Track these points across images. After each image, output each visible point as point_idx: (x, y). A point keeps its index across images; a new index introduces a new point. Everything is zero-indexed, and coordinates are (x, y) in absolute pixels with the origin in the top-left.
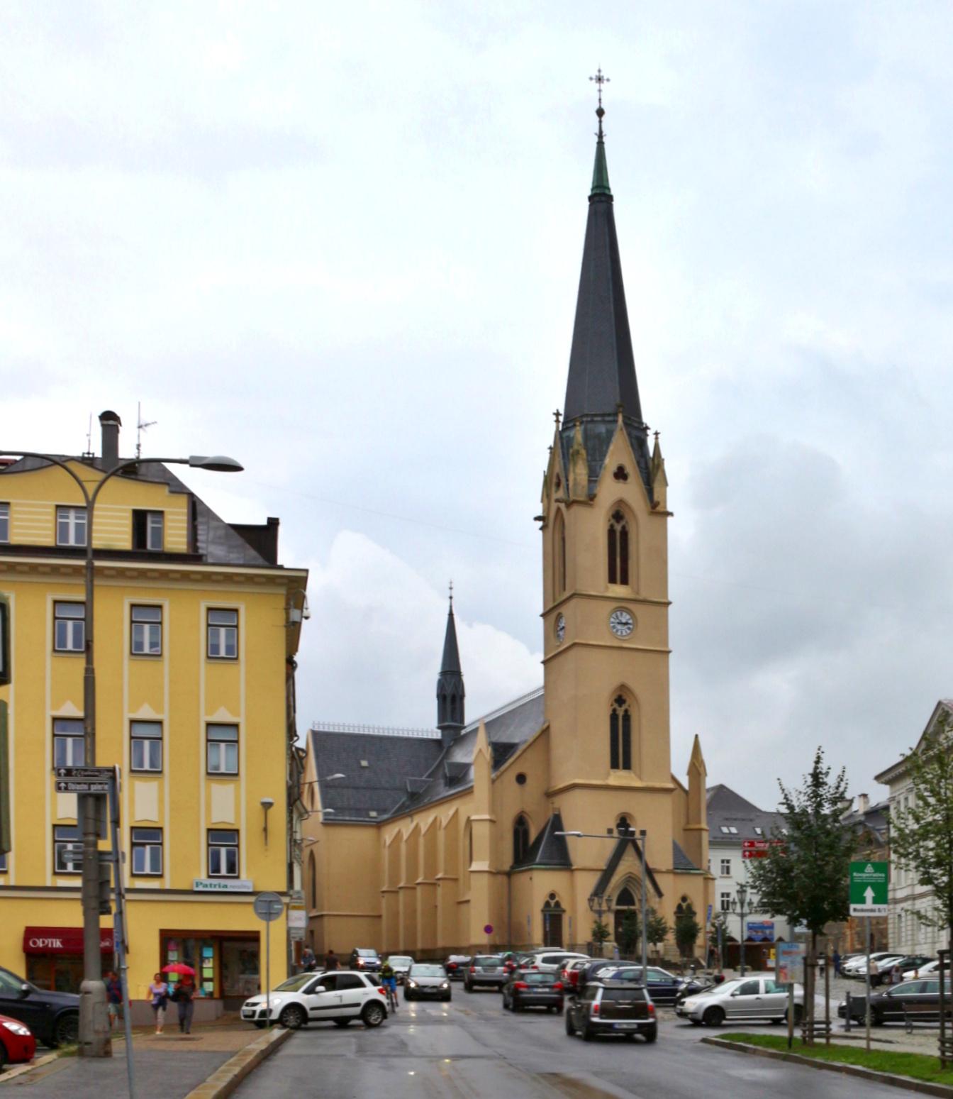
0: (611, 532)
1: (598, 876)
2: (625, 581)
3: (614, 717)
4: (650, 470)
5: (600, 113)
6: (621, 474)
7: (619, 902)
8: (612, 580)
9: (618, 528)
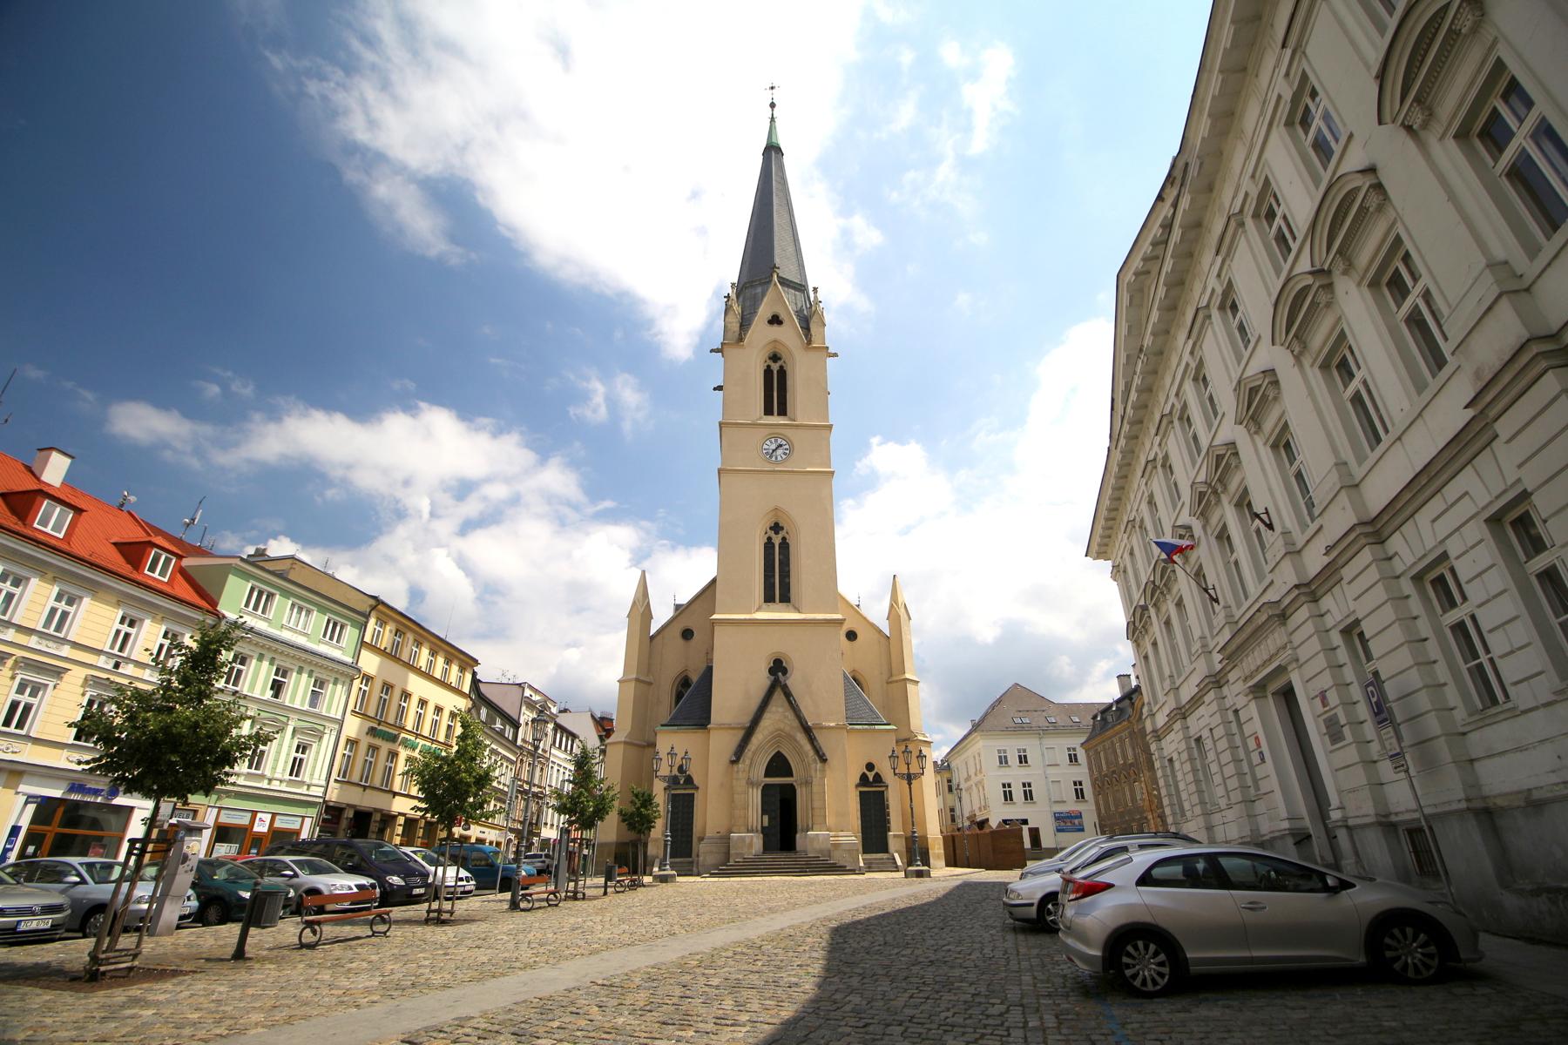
0: (768, 372)
1: (741, 734)
2: (783, 412)
3: (769, 546)
4: (809, 320)
5: (773, 105)
6: (775, 320)
7: (766, 775)
8: (768, 411)
9: (775, 367)
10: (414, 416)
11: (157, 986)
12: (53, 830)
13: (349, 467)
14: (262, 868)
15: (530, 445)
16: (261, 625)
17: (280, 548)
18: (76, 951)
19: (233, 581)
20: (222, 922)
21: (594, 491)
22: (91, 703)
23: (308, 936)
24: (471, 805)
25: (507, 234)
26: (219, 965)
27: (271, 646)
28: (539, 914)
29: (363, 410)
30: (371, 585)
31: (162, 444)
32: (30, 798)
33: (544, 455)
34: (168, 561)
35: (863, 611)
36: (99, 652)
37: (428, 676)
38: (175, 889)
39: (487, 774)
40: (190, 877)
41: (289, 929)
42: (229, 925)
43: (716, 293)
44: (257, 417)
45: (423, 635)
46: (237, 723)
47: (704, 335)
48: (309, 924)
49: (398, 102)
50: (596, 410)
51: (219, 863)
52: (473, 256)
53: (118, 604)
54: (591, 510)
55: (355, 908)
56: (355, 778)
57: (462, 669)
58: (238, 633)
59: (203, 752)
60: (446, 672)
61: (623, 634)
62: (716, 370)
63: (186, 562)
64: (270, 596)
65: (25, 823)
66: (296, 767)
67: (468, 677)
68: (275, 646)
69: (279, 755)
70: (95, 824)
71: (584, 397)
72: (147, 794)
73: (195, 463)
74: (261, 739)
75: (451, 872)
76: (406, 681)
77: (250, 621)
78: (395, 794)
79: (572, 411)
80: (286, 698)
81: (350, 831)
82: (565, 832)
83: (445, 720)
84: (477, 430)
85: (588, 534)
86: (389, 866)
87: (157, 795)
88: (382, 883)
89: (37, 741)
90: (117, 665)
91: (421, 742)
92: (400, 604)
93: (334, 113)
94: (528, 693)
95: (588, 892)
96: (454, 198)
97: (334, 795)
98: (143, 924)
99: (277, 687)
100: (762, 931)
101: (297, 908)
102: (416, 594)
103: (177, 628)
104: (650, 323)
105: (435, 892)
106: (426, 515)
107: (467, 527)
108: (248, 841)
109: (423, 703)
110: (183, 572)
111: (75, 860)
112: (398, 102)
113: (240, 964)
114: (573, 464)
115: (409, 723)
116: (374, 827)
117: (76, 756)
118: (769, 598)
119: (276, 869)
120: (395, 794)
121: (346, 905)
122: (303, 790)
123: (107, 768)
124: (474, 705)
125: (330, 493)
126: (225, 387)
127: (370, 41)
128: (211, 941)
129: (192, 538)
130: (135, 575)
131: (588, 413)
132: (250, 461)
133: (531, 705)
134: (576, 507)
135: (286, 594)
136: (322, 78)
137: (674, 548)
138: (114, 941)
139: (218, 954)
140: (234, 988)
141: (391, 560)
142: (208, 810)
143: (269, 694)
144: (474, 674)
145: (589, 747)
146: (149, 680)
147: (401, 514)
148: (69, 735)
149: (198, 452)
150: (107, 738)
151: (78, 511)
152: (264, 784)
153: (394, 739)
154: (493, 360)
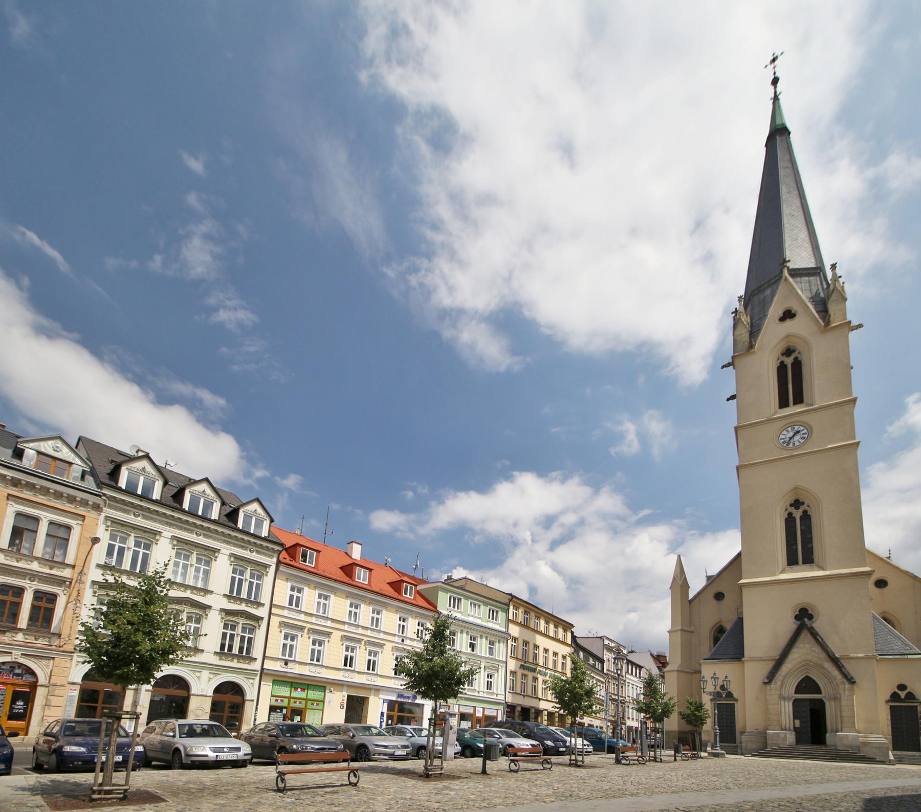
10: (512, 482)
11: (453, 782)
12: (396, 714)
13: (483, 522)
14: (485, 733)
15: (586, 483)
16: (459, 616)
17: (459, 573)
18: (418, 765)
19: (441, 594)
20: (473, 756)
21: (634, 505)
22: (397, 658)
23: (513, 766)
24: (585, 706)
25: (547, 331)
26: (476, 776)
27: (467, 626)
28: (634, 767)
29: (484, 486)
30: (507, 588)
31: (396, 529)
32: (384, 701)
33: (596, 488)
34: (411, 588)
35: (895, 561)
36: (395, 635)
37: (546, 635)
38: (450, 742)
39: (591, 689)
40: (455, 736)
41: (503, 762)
42: (476, 759)
43: (725, 312)
44: (433, 504)
45: (540, 613)
46: (460, 664)
47: (716, 355)
48: (513, 761)
49: (462, 264)
50: (631, 444)
51: (464, 730)
52: (529, 359)
53: (397, 612)
54: (634, 518)
55: (532, 755)
56: (518, 691)
57: (565, 631)
58: (450, 621)
59: (449, 679)
60: (556, 633)
61: (668, 601)
62: (729, 382)
63: (419, 588)
64: (459, 600)
65: (385, 711)
66: (489, 685)
67: (569, 635)
68: (467, 625)
69: (480, 680)
70: (410, 711)
71: (620, 437)
72: (431, 698)
73: (411, 536)
74: (472, 672)
75: (579, 741)
76: (535, 639)
77: (454, 614)
78: (540, 699)
79: (612, 450)
80: (478, 651)
81: (521, 717)
82: (643, 723)
83: (560, 660)
84: (551, 481)
85: (634, 536)
86: (545, 736)
87: (435, 699)
88: (543, 744)
89: (381, 676)
90: (403, 641)
91: (549, 672)
92: (524, 596)
93: (428, 292)
94: (606, 642)
95: (664, 758)
96: (511, 321)
97: (510, 699)
98: (441, 755)
99: (472, 646)
100: (801, 794)
101: (505, 753)
102: (533, 590)
103: (423, 621)
104: (668, 360)
105: (571, 751)
106: (530, 542)
107: (555, 545)
108: (475, 720)
109: (546, 651)
110: (418, 592)
111: (408, 727)
112: (462, 264)
113: (485, 776)
114: (618, 489)
115: (541, 661)
116: (532, 716)
117: (397, 682)
118: (792, 561)
119: (491, 734)
120: (540, 699)
121: (527, 754)
122: (495, 697)
123: (413, 687)
124: (575, 651)
125: (477, 539)
126: (414, 490)
127: (436, 226)
128: (470, 765)
129: (418, 575)
130: (400, 597)
131: (625, 448)
132: (435, 530)
133: (610, 649)
134: (622, 519)
135: (467, 598)
136: (417, 270)
137: (702, 535)
138: (432, 762)
139: (474, 771)
140: (486, 786)
141: (515, 572)
142: (455, 706)
143: (469, 650)
144: (572, 633)
145: (653, 674)
146: (419, 647)
147: (515, 544)
148: (392, 674)
149: (411, 530)
150: (409, 674)
151: (370, 570)
152: (476, 694)
153: (534, 670)
154: (554, 430)
